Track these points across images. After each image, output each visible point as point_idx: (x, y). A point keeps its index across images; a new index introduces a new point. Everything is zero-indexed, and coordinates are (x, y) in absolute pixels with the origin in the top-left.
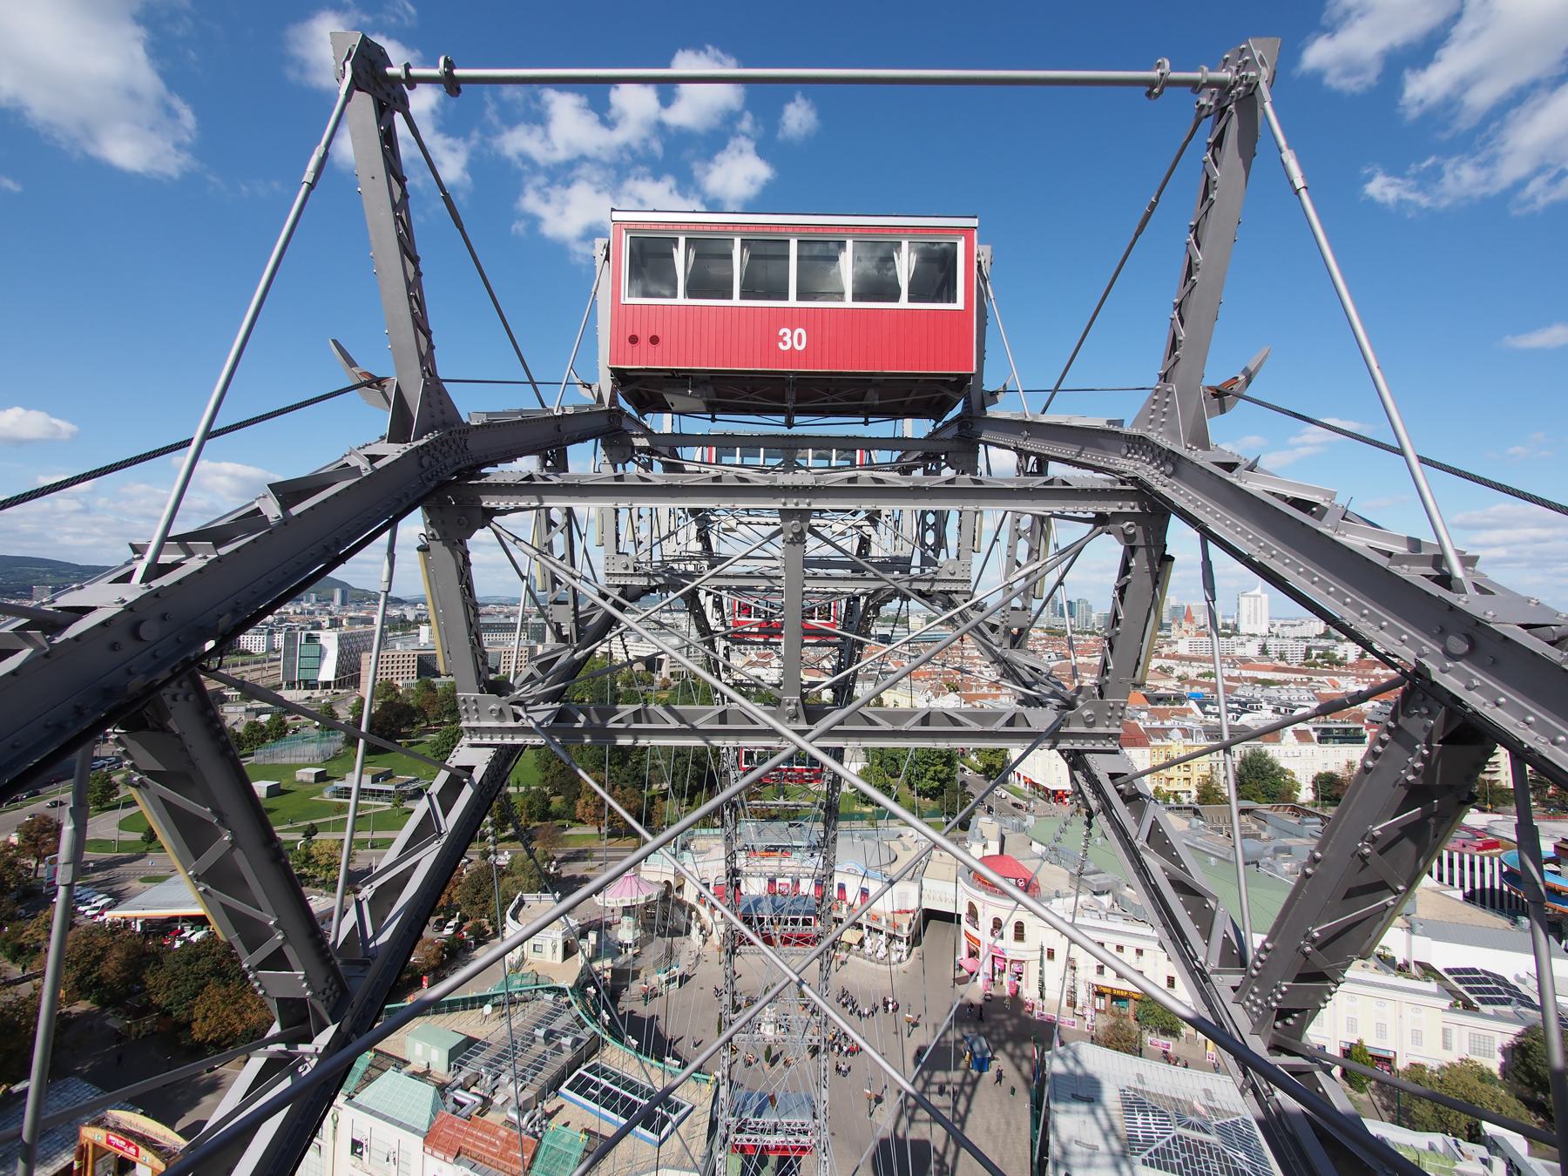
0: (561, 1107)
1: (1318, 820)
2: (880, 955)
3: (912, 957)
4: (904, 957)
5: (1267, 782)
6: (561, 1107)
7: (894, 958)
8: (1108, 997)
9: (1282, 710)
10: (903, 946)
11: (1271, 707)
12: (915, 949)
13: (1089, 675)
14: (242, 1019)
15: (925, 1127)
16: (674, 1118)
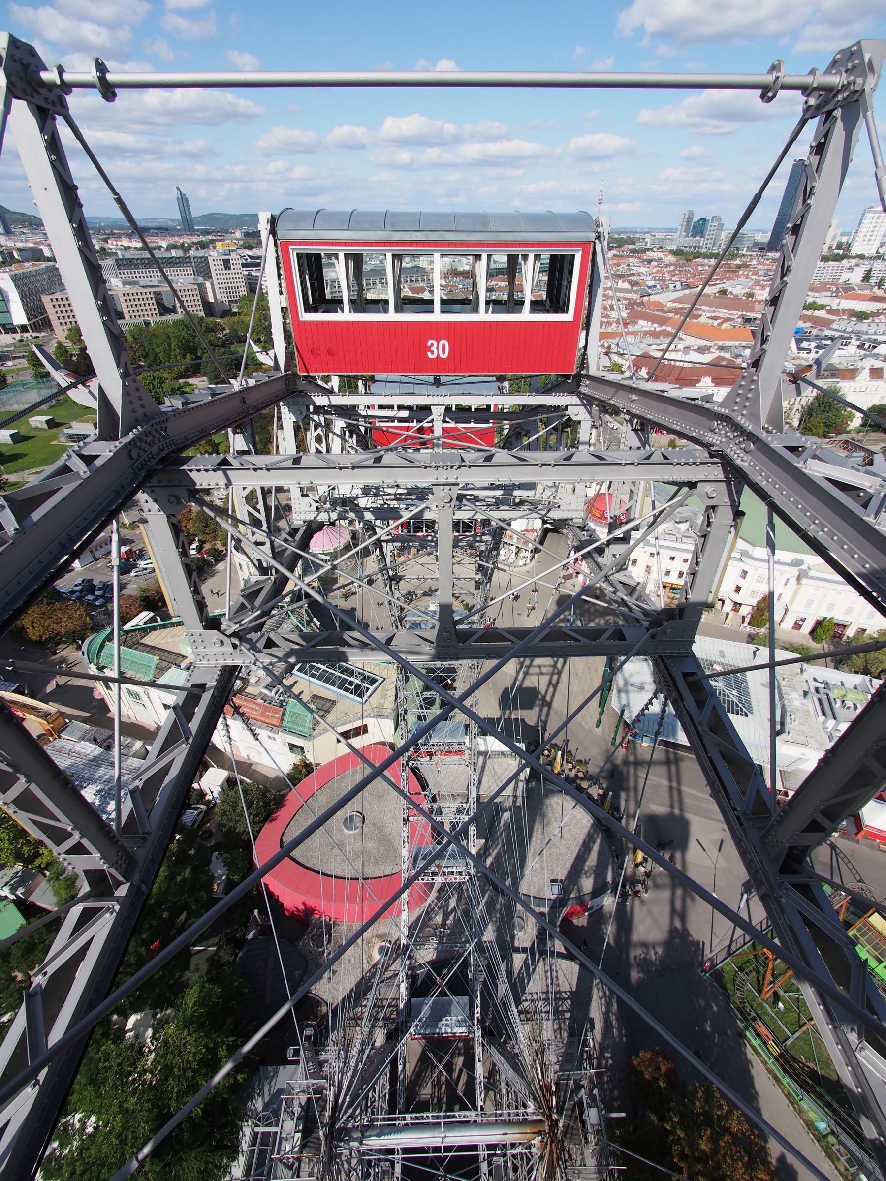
0: (296, 682)
1: (863, 454)
2: (511, 561)
3: (533, 561)
4: (528, 561)
5: (830, 414)
6: (296, 682)
7: (521, 563)
8: (668, 589)
9: (866, 346)
10: (529, 554)
11: (858, 343)
12: (536, 555)
13: (707, 308)
14: (61, 627)
15: (534, 678)
16: (372, 688)
